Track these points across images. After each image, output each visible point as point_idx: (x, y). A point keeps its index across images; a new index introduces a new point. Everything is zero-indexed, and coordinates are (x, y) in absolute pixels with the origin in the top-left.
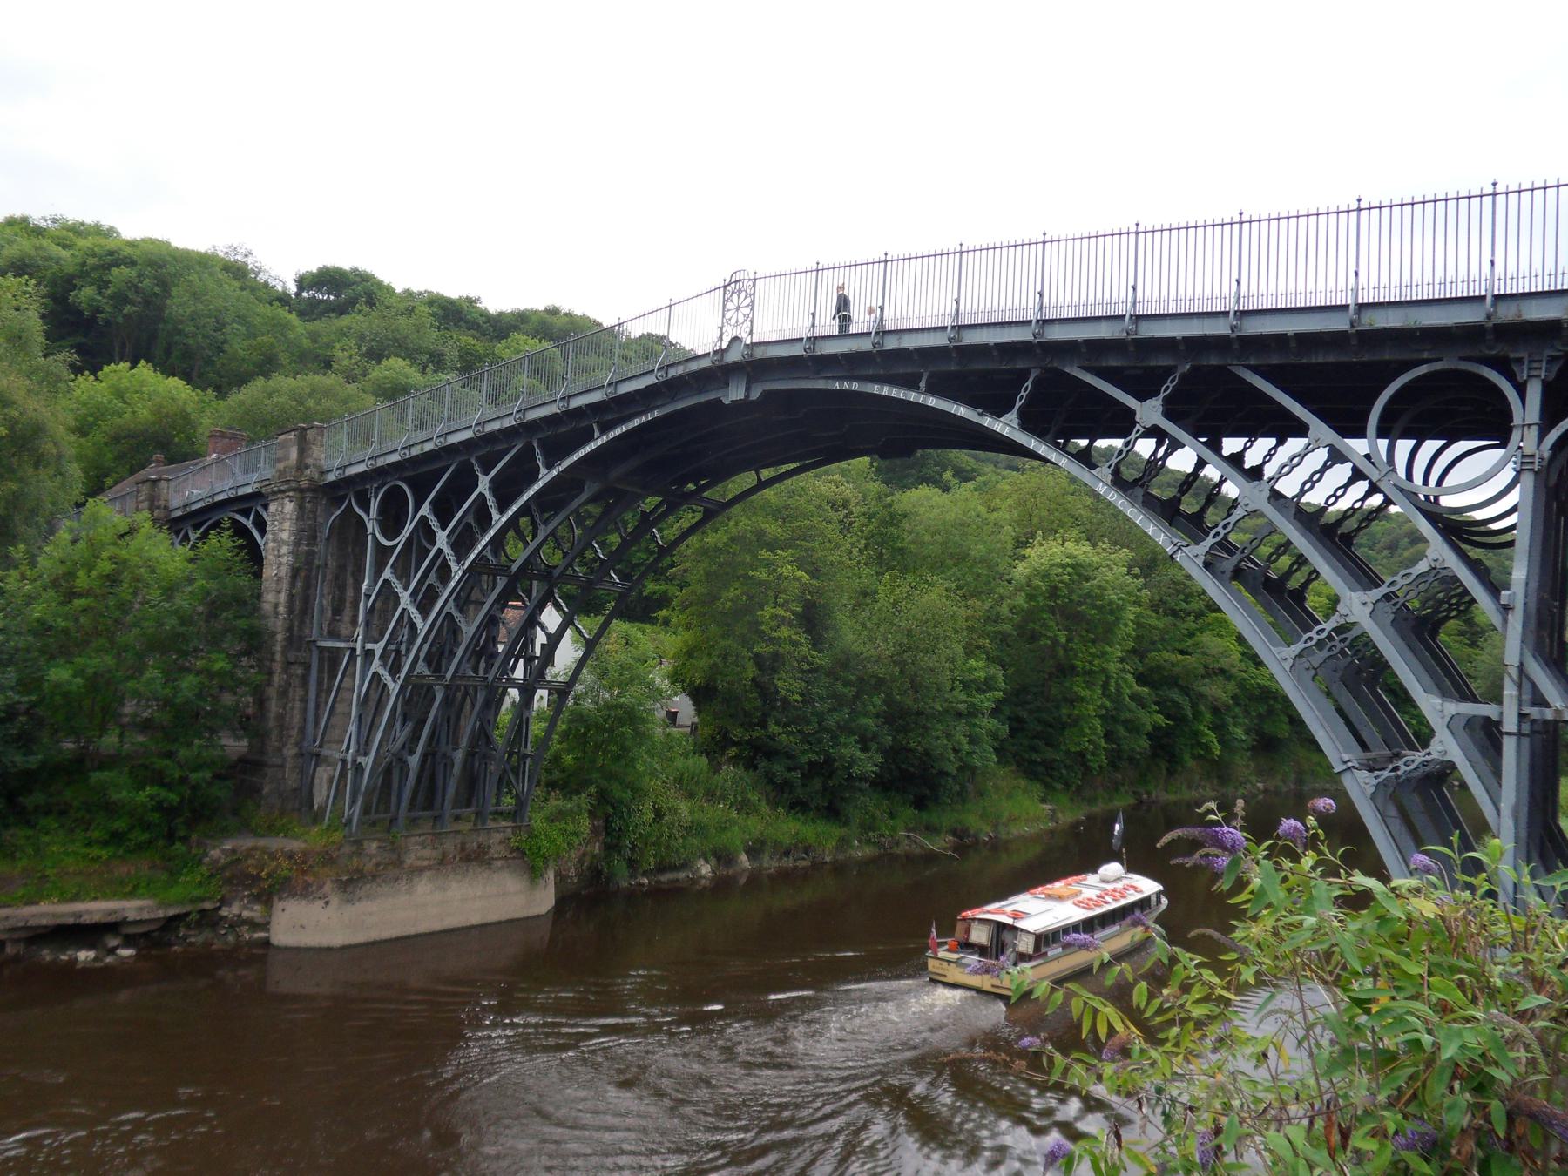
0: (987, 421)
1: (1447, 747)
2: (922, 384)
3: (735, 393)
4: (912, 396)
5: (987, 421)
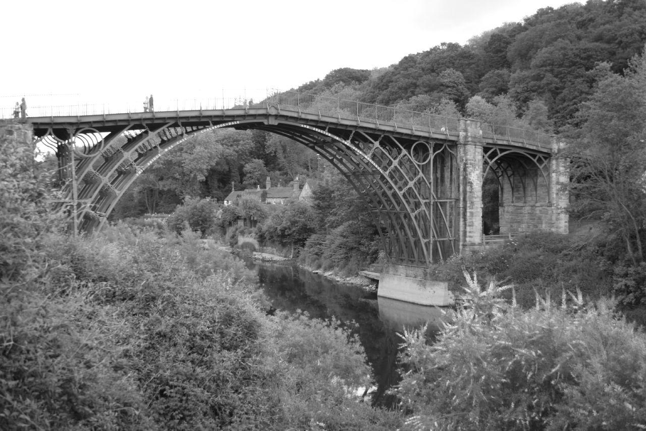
0: (343, 141)
1: (423, 208)
2: (327, 130)
3: (273, 122)
4: (324, 133)
5: (343, 141)
